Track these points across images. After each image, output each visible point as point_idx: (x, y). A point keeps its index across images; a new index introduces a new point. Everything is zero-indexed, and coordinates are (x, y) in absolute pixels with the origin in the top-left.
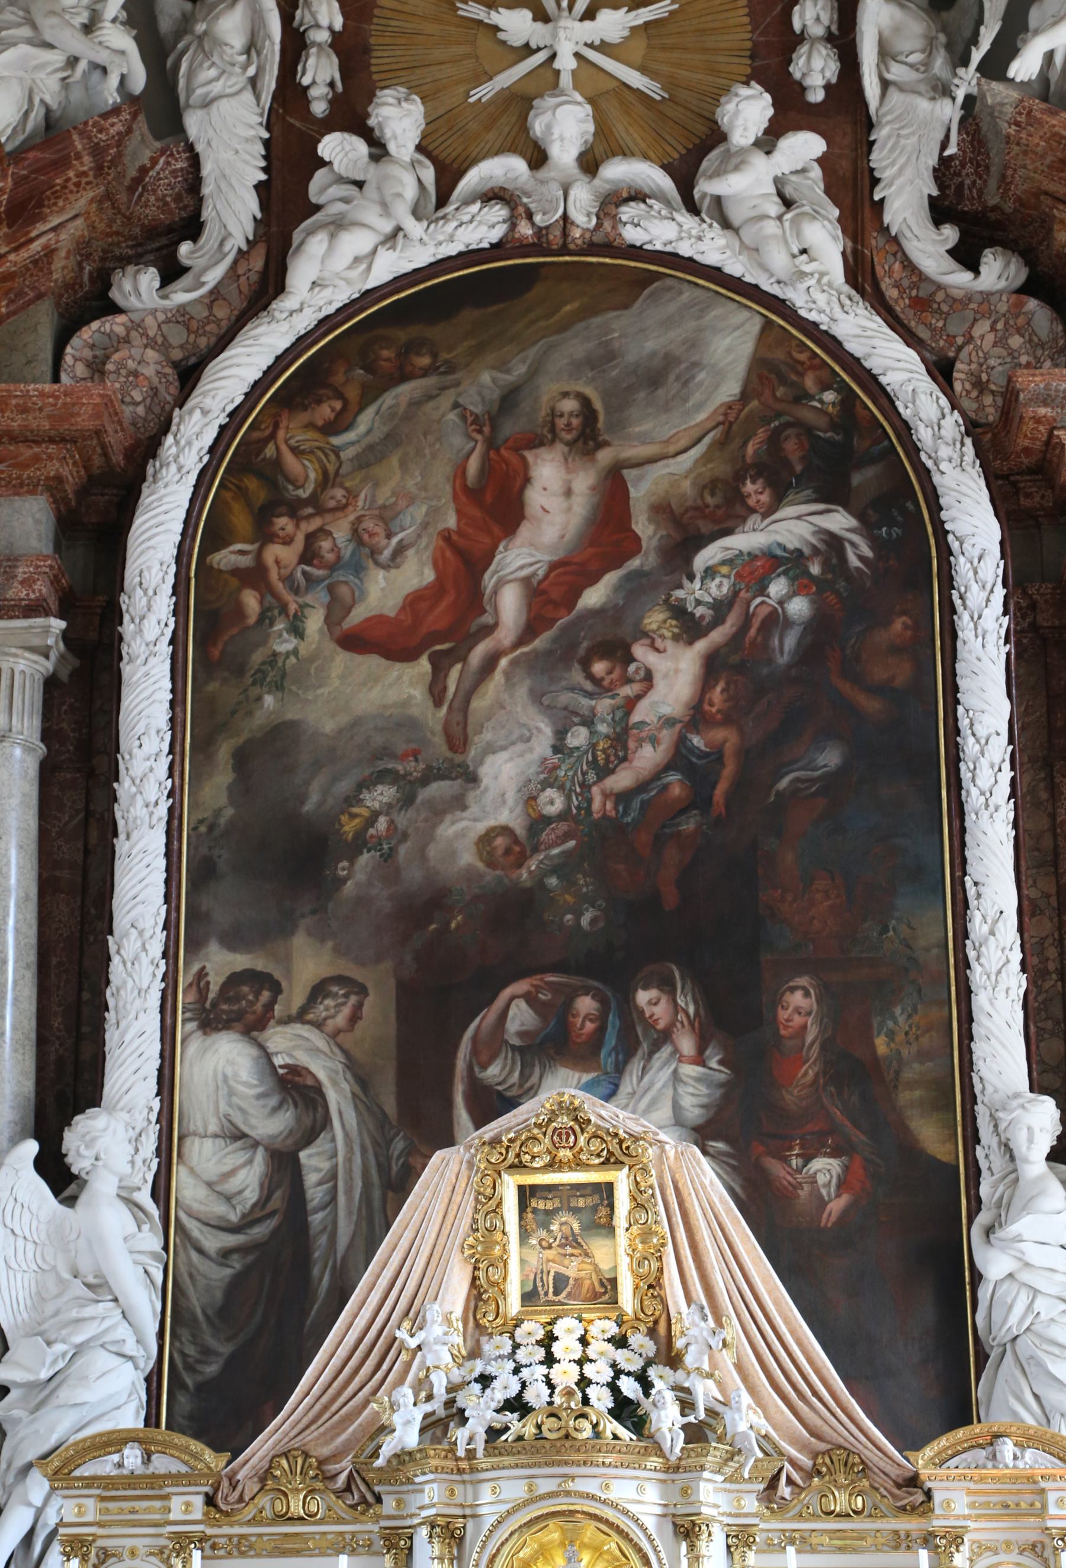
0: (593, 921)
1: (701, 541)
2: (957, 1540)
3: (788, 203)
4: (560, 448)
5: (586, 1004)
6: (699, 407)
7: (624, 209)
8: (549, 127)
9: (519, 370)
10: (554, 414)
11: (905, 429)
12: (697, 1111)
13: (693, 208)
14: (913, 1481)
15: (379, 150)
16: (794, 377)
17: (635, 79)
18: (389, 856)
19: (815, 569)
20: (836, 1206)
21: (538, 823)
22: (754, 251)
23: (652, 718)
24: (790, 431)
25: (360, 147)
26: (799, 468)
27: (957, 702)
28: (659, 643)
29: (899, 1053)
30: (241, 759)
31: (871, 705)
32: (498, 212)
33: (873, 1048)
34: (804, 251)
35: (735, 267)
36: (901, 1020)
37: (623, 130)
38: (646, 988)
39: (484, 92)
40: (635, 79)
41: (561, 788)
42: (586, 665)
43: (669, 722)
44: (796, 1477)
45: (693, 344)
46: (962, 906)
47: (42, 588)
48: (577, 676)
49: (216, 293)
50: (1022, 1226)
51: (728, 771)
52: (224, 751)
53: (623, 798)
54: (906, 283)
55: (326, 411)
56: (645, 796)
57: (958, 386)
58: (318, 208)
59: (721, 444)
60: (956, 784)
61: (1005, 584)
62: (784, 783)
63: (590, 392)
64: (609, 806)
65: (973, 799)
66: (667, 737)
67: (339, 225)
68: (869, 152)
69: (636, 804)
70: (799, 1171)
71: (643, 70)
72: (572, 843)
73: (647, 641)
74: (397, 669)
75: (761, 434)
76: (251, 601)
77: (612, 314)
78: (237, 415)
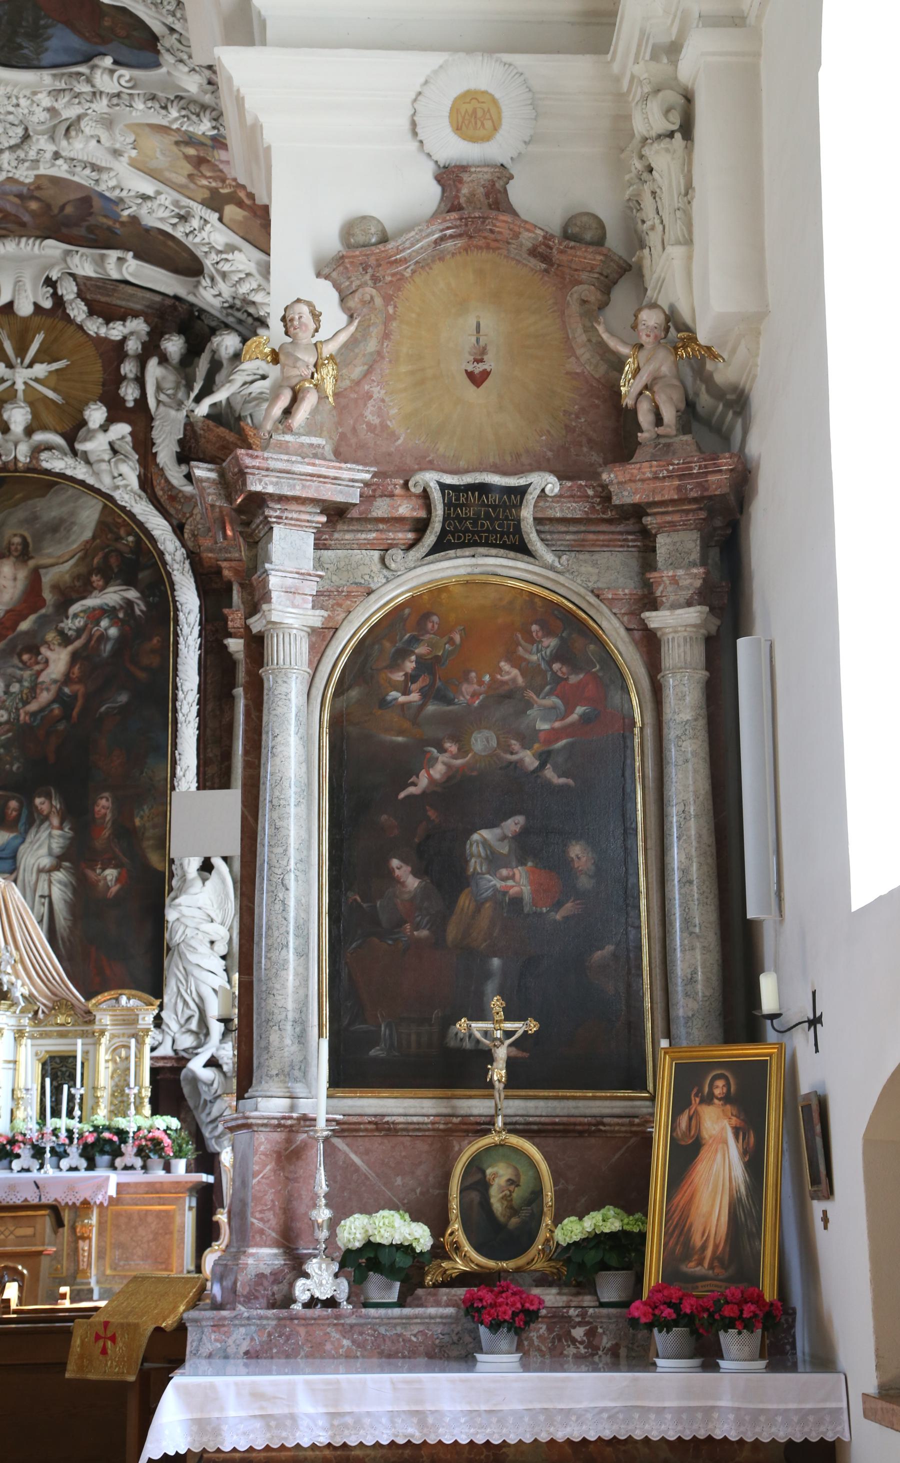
0: (18, 768)
1: (73, 602)
2: (102, 1033)
3: (115, 451)
4: (12, 559)
5: (13, 804)
6: (74, 541)
7: (42, 454)
8: (9, 417)
10: (10, 544)
11: (161, 554)
12: (58, 850)
13: (75, 453)
14: (89, 1012)
16: (115, 530)
17: (51, 394)
19: (121, 615)
20: (114, 889)
22: (96, 474)
23: (47, 680)
24: (113, 554)
26: (116, 570)
27: (177, 676)
28: (52, 647)
29: (144, 825)
31: (142, 675)
33: (134, 823)
34: (121, 475)
35: (91, 481)
36: (147, 811)
38: (39, 797)
40: (51, 394)
41: (7, 710)
42: (20, 656)
43: (55, 681)
44: (45, 1010)
45: (72, 514)
46: (174, 763)
48: (16, 661)
50: (182, 900)
53: (33, 715)
54: (166, 489)
56: (43, 714)
57: (186, 536)
59: (82, 559)
60: (175, 711)
61: (200, 624)
62: (103, 709)
63: (26, 534)
64: (27, 718)
68: (151, 430)
69: (39, 717)
70: (100, 875)
71: (54, 390)
72: (10, 734)
73: (46, 646)
75: (100, 555)
77: (37, 499)
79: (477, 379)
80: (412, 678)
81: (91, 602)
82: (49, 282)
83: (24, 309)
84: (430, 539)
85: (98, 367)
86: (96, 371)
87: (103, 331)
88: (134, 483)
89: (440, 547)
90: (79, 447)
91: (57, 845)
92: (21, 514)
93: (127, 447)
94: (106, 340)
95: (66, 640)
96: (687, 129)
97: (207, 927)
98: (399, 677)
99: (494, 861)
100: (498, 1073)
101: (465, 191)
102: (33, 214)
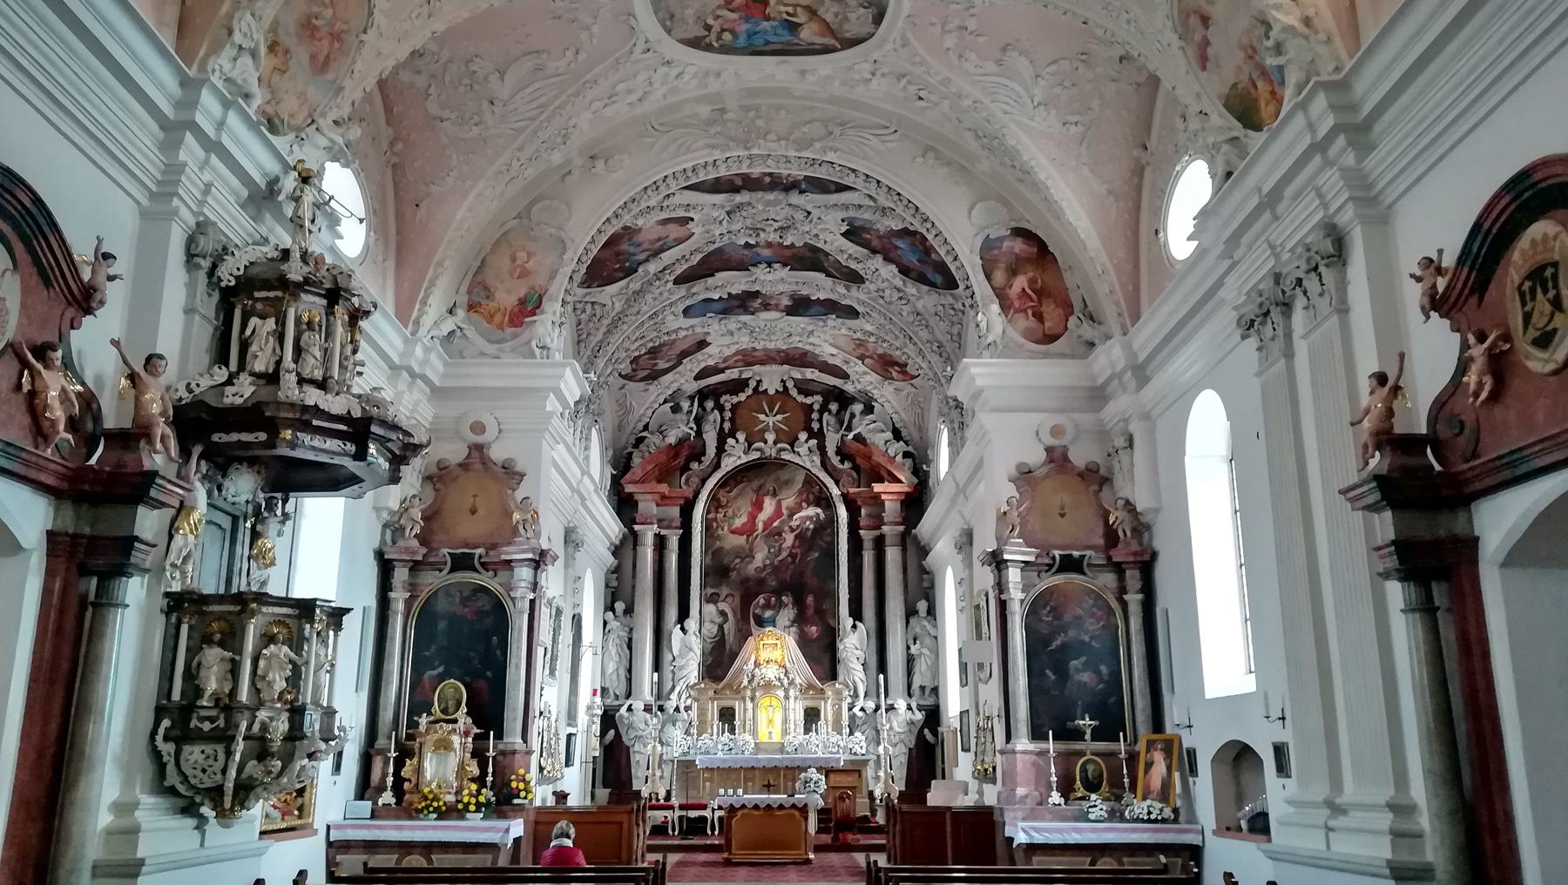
3: (811, 451)
9: (762, 481)
13: (794, 452)
15: (737, 441)
17: (783, 427)
18: (739, 571)
21: (765, 566)
25: (734, 441)
30: (713, 554)
32: (759, 453)
35: (801, 463)
37: (783, 437)
39: (756, 429)
40: (783, 427)
47: (679, 524)
51: (799, 557)
55: (728, 489)
67: (730, 455)
76: (715, 524)
78: (712, 490)
79: (1062, 515)
80: (1049, 612)
81: (803, 514)
82: (783, 381)
83: (771, 392)
84: (1054, 569)
86: (801, 416)
89: (1057, 572)
90: (796, 449)
91: (792, 618)
92: (773, 477)
93: (815, 449)
95: (792, 530)
96: (1131, 446)
97: (856, 652)
98: (1045, 612)
99: (1078, 671)
100: (1088, 737)
101: (1055, 454)
102: (781, 357)
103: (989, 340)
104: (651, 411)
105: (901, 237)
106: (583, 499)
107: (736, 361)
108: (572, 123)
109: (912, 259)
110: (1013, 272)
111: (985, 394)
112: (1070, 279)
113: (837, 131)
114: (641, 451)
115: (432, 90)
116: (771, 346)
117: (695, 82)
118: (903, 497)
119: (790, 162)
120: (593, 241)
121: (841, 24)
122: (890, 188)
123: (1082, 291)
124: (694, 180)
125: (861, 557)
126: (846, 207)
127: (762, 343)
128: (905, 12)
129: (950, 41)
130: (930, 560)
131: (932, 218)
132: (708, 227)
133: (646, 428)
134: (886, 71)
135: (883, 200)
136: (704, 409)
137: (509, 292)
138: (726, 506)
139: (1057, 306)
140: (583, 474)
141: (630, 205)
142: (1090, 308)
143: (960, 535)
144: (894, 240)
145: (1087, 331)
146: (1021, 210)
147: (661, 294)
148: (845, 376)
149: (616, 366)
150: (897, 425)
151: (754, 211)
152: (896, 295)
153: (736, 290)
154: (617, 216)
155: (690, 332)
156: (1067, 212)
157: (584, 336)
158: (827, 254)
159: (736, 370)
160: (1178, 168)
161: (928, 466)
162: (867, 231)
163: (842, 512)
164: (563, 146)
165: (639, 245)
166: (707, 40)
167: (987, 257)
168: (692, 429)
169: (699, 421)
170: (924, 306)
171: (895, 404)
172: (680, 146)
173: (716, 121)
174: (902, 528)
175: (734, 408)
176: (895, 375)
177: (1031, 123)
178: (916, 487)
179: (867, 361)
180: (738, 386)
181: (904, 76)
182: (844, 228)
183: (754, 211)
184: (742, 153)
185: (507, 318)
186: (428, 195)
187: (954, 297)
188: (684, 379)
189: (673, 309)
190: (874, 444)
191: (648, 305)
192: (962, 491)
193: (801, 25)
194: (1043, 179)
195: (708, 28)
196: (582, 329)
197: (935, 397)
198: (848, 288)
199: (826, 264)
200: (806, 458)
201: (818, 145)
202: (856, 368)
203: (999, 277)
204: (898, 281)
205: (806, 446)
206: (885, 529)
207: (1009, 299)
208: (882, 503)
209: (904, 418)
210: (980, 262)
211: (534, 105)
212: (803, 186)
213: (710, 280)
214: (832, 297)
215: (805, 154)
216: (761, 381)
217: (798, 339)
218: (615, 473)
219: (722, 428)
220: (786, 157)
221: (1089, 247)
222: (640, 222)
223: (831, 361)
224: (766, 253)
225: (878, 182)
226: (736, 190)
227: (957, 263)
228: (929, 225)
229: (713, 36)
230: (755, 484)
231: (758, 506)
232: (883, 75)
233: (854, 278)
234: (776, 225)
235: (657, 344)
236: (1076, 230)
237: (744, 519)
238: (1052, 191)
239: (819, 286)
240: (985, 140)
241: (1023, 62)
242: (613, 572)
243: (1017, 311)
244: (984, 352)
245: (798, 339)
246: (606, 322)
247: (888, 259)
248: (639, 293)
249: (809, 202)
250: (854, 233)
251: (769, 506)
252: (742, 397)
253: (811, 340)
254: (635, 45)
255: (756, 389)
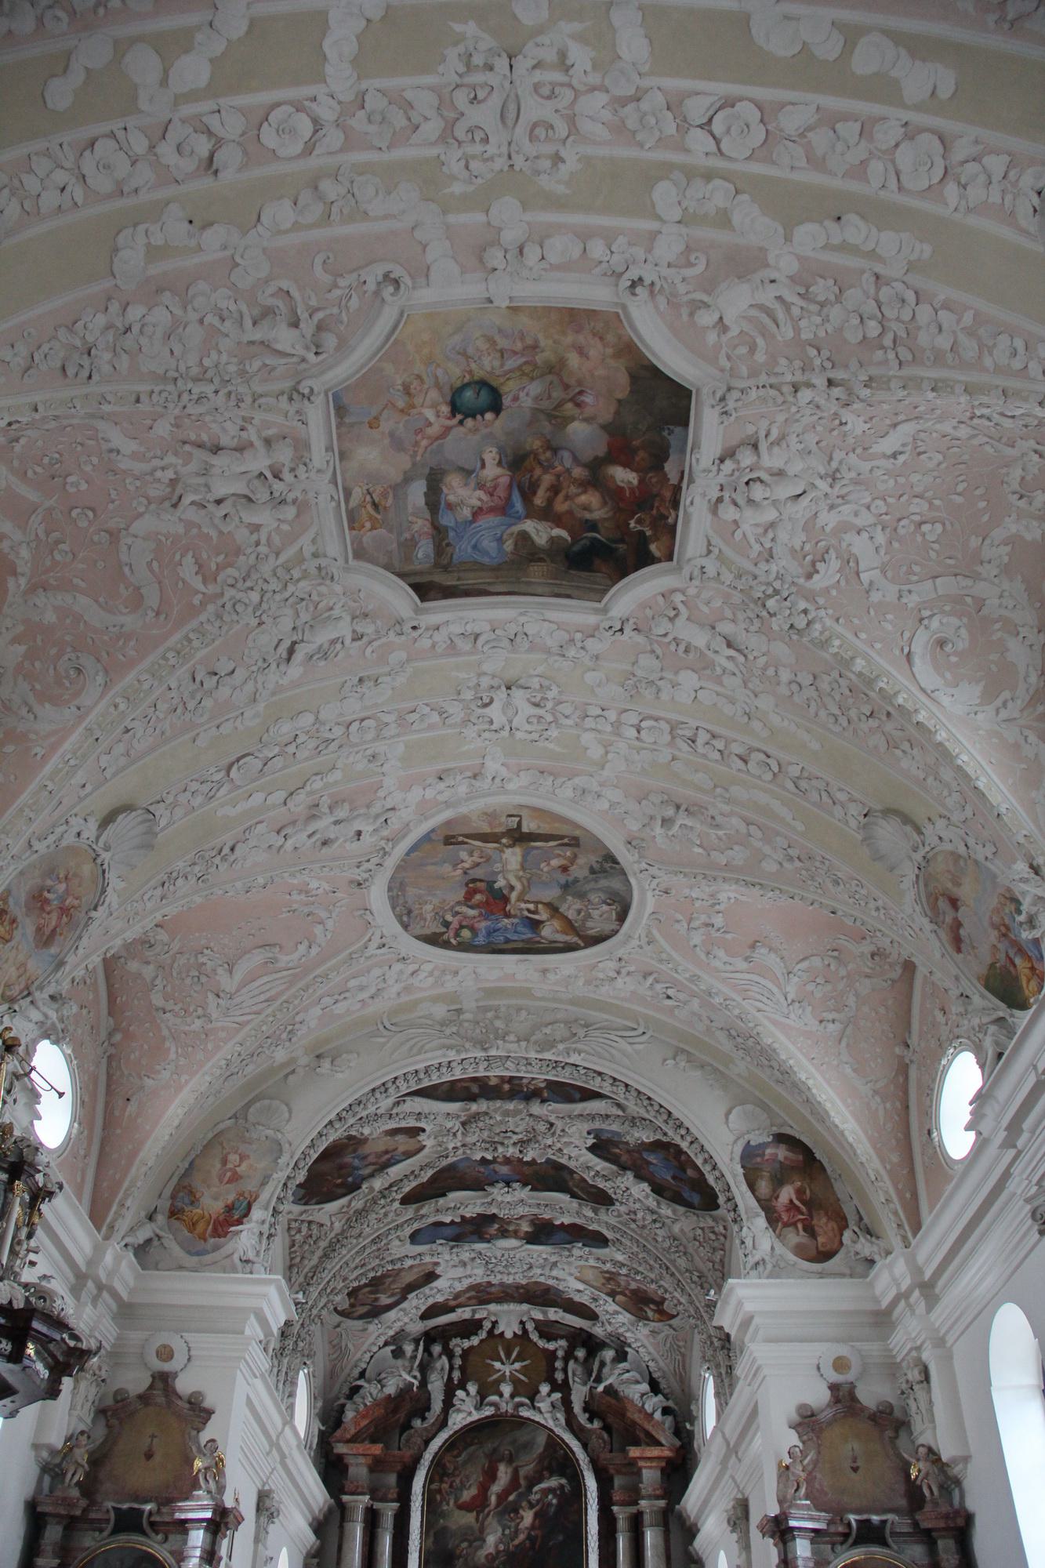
9: (495, 1445)
11: (577, 1460)
13: (534, 1407)
15: (468, 1394)
18: (466, 1560)
21: (498, 1552)
32: (493, 1408)
35: (543, 1422)
47: (395, 1496)
49: (433, 1424)
52: (432, 1533)
53: (517, 1547)
55: (455, 1452)
58: (454, 1405)
65: (590, 1550)
66: (526, 1532)
67: (459, 1411)
74: (469, 1514)
76: (438, 1497)
78: (436, 1454)
81: (543, 1485)
83: (509, 1335)
85: (544, 1363)
87: (546, 1346)
88: (563, 1421)
93: (559, 1404)
94: (547, 1350)
95: (531, 1506)
103: (757, 1258)
104: (368, 1355)
105: (653, 1151)
106: (283, 1456)
107: (469, 1298)
108: (298, 1019)
109: (666, 1176)
110: (778, 1182)
111: (756, 1321)
112: (841, 1189)
113: (581, 1032)
114: (355, 1403)
115: (157, 982)
116: (509, 1280)
117: (431, 980)
118: (664, 1464)
119: (530, 1064)
120: (312, 1145)
121: (584, 920)
122: (639, 1092)
123: (856, 1201)
124: (426, 1083)
125: (615, 1541)
126: (592, 1117)
127: (499, 1276)
128: (649, 909)
129: (697, 938)
130: (699, 1543)
131: (687, 1124)
132: (440, 1139)
133: (362, 1375)
134: (632, 969)
135: (634, 1108)
136: (430, 1354)
137: (216, 1198)
138: (453, 1475)
139: (829, 1219)
140: (284, 1424)
141: (356, 1108)
142: (866, 1220)
143: (734, 1507)
144: (645, 1155)
145: (865, 1247)
146: (782, 1114)
147: (386, 1215)
148: (592, 1316)
149: (331, 1297)
150: (655, 1375)
151: (492, 1122)
152: (649, 1218)
153: (470, 1212)
154: (340, 1119)
155: (417, 1262)
156: (832, 1114)
157: (298, 1260)
158: (572, 1172)
159: (468, 1309)
160: (944, 1062)
161: (692, 1424)
162: (616, 1144)
163: (591, 1484)
164: (287, 1044)
165: (365, 1157)
166: (445, 937)
167: (748, 1166)
168: (415, 1377)
169: (424, 1368)
170: (682, 1230)
171: (651, 1349)
172: (411, 1048)
173: (451, 1021)
174: (662, 1503)
175: (466, 1354)
176: (650, 1314)
177: (787, 1021)
178: (678, 1450)
179: (619, 1298)
180: (470, 1327)
181: (650, 974)
182: (591, 1141)
183: (492, 1122)
184: (480, 1054)
185: (211, 1227)
186: (142, 1088)
187: (715, 1219)
188: (407, 1317)
189: (399, 1233)
190: (627, 1398)
191: (370, 1228)
192: (733, 1450)
193: (542, 922)
194: (803, 1079)
195: (447, 924)
196: (295, 1252)
197: (697, 1337)
198: (595, 1211)
199: (571, 1184)
200: (547, 1415)
201: (561, 1047)
202: (607, 1307)
203: (764, 1186)
204: (651, 1201)
205: (549, 1400)
206: (643, 1503)
207: (776, 1212)
208: (639, 1473)
209: (660, 1365)
210: (741, 1171)
211: (262, 997)
212: (546, 1095)
213: (441, 1201)
214: (578, 1221)
215: (547, 1056)
216: (496, 1322)
217: (539, 1271)
218: (323, 1428)
219: (450, 1378)
220: (527, 1059)
221: (859, 1152)
222: (366, 1131)
223: (577, 1298)
224: (504, 1170)
225: (627, 1085)
226: (473, 1098)
227: (717, 1173)
228: (683, 1132)
229: (451, 933)
230: (489, 1446)
231: (491, 1476)
232: (629, 973)
233: (602, 1199)
234: (515, 1138)
235: (379, 1274)
236: (842, 1133)
237: (474, 1491)
238: (814, 1091)
239: (564, 1209)
240: (740, 1040)
241: (773, 961)
242: (314, 1557)
243: (786, 1225)
244: (751, 1273)
245: (539, 1271)
246: (323, 1244)
247: (640, 1177)
248: (361, 1213)
249: (552, 1112)
250: (602, 1147)
251: (504, 1473)
252: (475, 1341)
253: (554, 1273)
254: (370, 940)
255: (490, 1332)
